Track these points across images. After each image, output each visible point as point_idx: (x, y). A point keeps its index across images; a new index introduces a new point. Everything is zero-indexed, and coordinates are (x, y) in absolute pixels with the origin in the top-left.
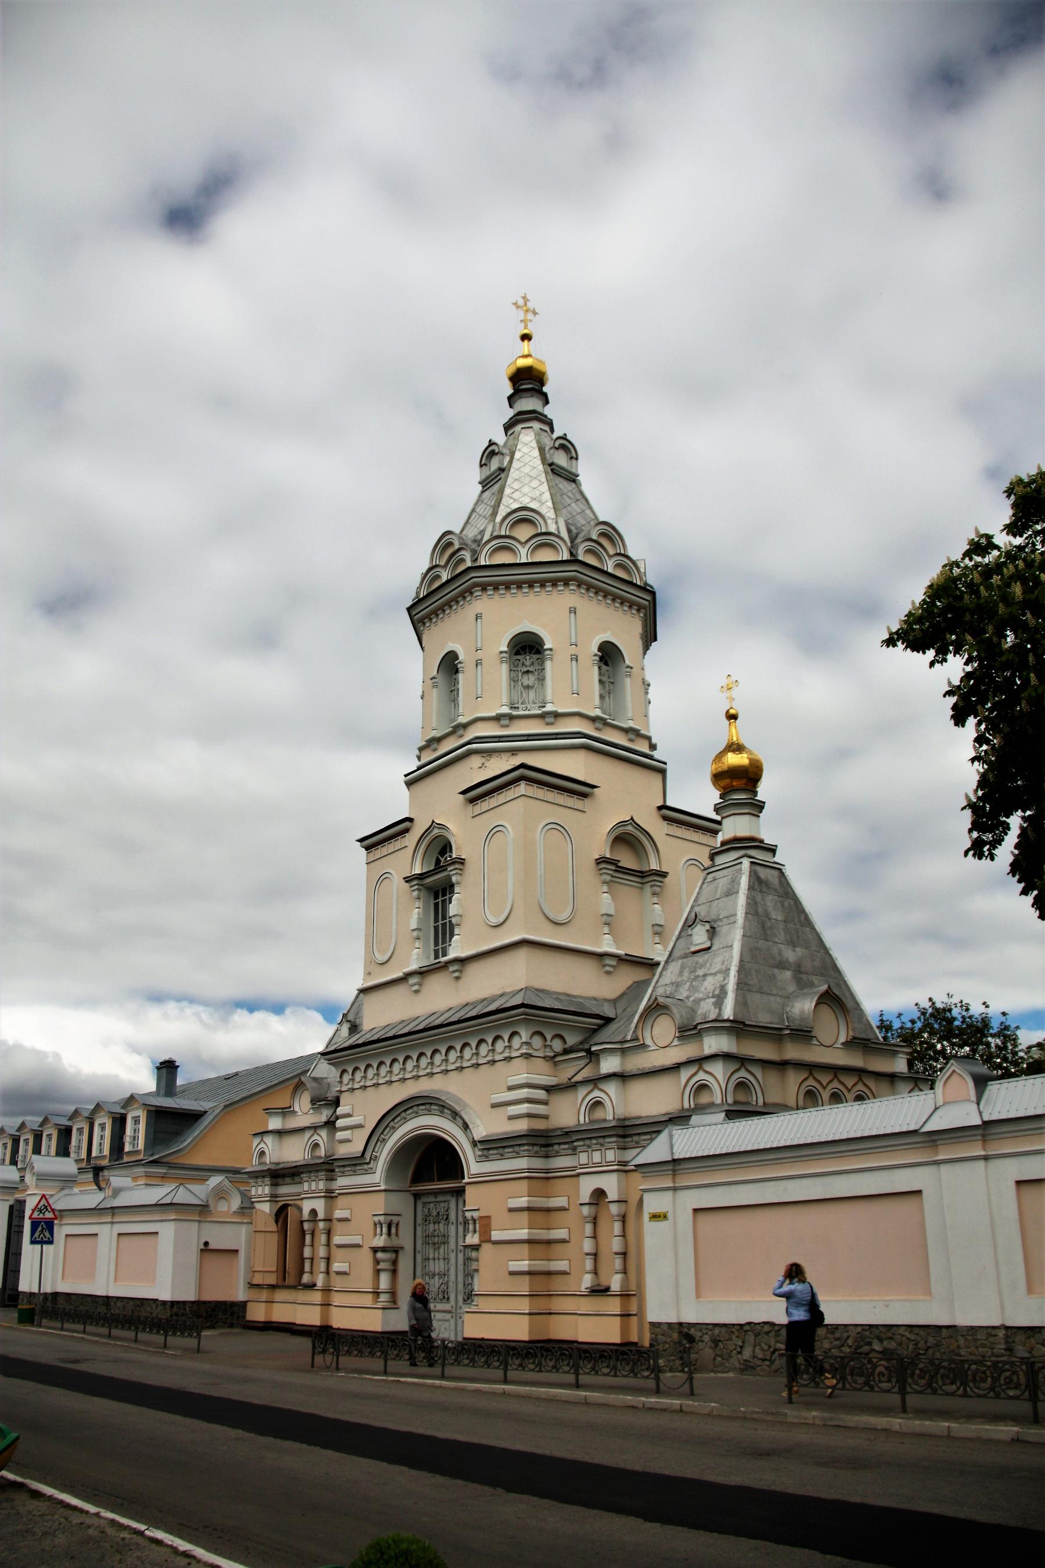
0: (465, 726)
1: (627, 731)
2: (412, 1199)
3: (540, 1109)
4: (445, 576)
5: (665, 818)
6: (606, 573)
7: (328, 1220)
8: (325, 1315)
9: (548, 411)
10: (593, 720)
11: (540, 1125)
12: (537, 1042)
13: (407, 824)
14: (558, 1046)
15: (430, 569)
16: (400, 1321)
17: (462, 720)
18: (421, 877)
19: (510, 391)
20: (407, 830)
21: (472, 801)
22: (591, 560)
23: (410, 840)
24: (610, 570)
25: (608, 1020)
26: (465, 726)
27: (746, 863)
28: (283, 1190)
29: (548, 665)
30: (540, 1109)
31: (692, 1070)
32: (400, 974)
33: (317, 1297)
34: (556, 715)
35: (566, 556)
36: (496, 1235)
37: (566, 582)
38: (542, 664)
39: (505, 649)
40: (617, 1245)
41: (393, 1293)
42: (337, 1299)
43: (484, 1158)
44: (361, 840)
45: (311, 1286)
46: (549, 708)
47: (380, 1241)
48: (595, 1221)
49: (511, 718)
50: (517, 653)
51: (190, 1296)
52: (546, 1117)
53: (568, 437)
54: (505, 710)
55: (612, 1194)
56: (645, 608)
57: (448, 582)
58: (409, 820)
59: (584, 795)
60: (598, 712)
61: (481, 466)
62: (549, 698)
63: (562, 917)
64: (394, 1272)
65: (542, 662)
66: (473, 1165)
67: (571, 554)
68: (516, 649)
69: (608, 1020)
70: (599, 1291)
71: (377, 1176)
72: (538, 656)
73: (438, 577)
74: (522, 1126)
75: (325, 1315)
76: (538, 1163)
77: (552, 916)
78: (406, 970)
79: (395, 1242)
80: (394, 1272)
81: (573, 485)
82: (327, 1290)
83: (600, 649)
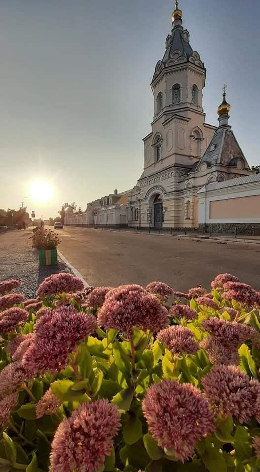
2: (153, 205)
3: (177, 187)
6: (195, 65)
7: (140, 210)
8: (140, 225)
10: (191, 104)
11: (177, 190)
14: (181, 174)
15: (155, 72)
16: (152, 225)
17: (162, 108)
21: (164, 126)
24: (196, 64)
25: (191, 169)
27: (225, 130)
28: (133, 205)
29: (181, 91)
30: (177, 187)
31: (210, 174)
33: (138, 222)
34: (182, 103)
35: (186, 61)
36: (168, 210)
40: (191, 211)
41: (151, 221)
42: (142, 222)
43: (167, 196)
45: (138, 220)
46: (181, 102)
47: (148, 213)
48: (187, 207)
51: (119, 223)
54: (171, 104)
55: (191, 201)
57: (159, 74)
58: (152, 133)
59: (188, 121)
64: (151, 217)
69: (191, 169)
70: (188, 219)
71: (147, 202)
74: (174, 190)
75: (140, 225)
80: (151, 217)
82: (140, 221)
83: (193, 86)
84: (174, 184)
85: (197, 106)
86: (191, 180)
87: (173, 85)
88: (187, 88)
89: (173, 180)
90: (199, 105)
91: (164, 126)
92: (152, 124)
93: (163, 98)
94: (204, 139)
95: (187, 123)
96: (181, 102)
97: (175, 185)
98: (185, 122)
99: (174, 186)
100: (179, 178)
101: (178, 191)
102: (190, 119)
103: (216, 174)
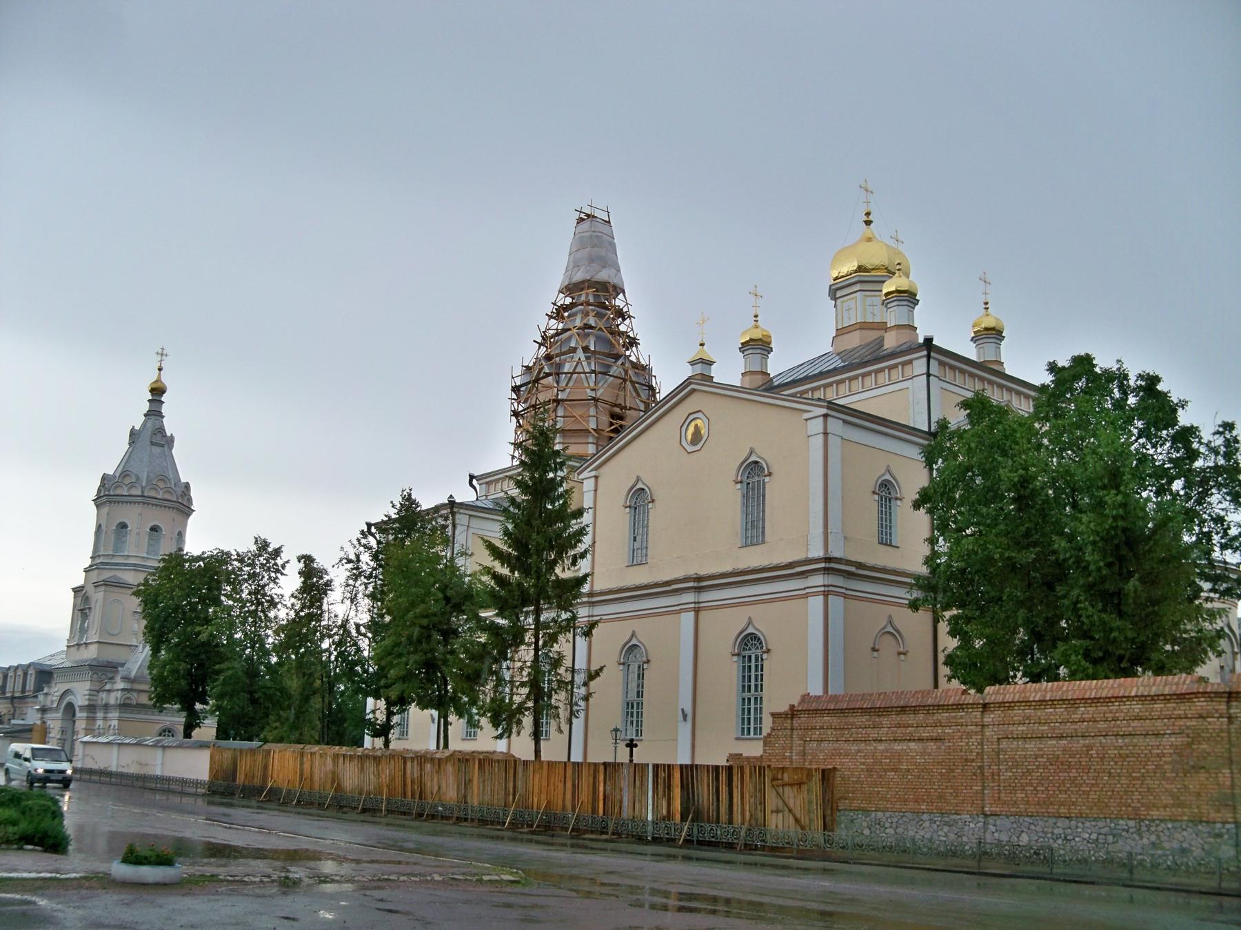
0: (99, 556)
3: (95, 698)
11: (94, 703)
12: (95, 676)
18: (82, 610)
22: (152, 494)
24: (159, 497)
26: (99, 556)
30: (95, 698)
34: (128, 556)
37: (139, 503)
43: (80, 712)
47: (58, 737)
49: (113, 556)
52: (96, 700)
54: (111, 553)
58: (83, 587)
66: (78, 714)
71: (59, 715)
74: (86, 703)
76: (91, 715)
77: (111, 632)
79: (64, 737)
84: (88, 692)
86: (105, 693)
88: (138, 534)
89: (87, 685)
93: (103, 536)
97: (90, 695)
99: (87, 697)
100: (97, 684)
101: (91, 708)
103: (120, 692)
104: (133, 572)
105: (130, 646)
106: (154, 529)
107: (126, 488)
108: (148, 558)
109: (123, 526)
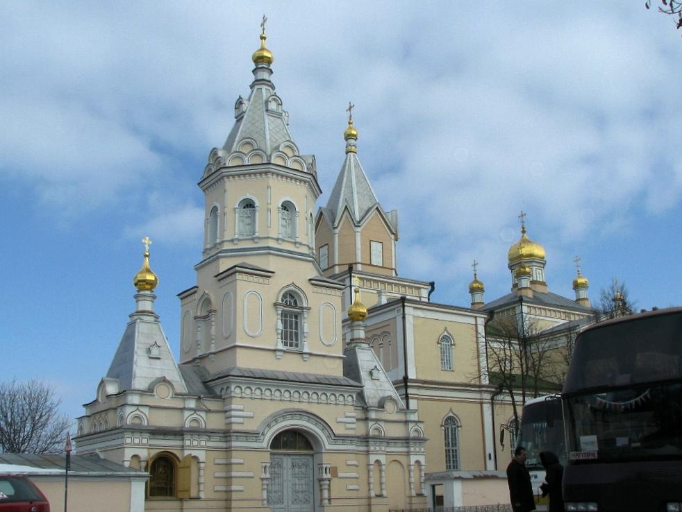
1: (295, 243)
4: (213, 170)
5: (313, 284)
9: (273, 79)
10: (277, 239)
13: (196, 289)
15: (208, 165)
19: (253, 66)
20: (195, 292)
21: (219, 280)
23: (197, 296)
29: (257, 214)
32: (191, 359)
34: (259, 238)
37: (266, 173)
38: (255, 213)
39: (237, 206)
44: (178, 295)
46: (257, 235)
50: (244, 208)
53: (277, 95)
56: (308, 182)
57: (215, 172)
58: (197, 287)
59: (269, 277)
60: (280, 237)
61: (236, 108)
62: (257, 230)
63: (256, 334)
65: (254, 212)
67: (267, 160)
68: (243, 206)
72: (252, 209)
73: (210, 169)
77: (251, 334)
78: (194, 357)
81: (279, 121)
85: (295, 243)
87: (241, 199)
88: (269, 210)
90: (298, 240)
91: (219, 280)
92: (200, 267)
94: (309, 309)
95: (266, 281)
96: (257, 235)
98: (261, 280)
102: (273, 272)
104: (271, 257)
105: (275, 351)
106: (287, 206)
107: (246, 159)
108: (283, 240)
109: (249, 204)
